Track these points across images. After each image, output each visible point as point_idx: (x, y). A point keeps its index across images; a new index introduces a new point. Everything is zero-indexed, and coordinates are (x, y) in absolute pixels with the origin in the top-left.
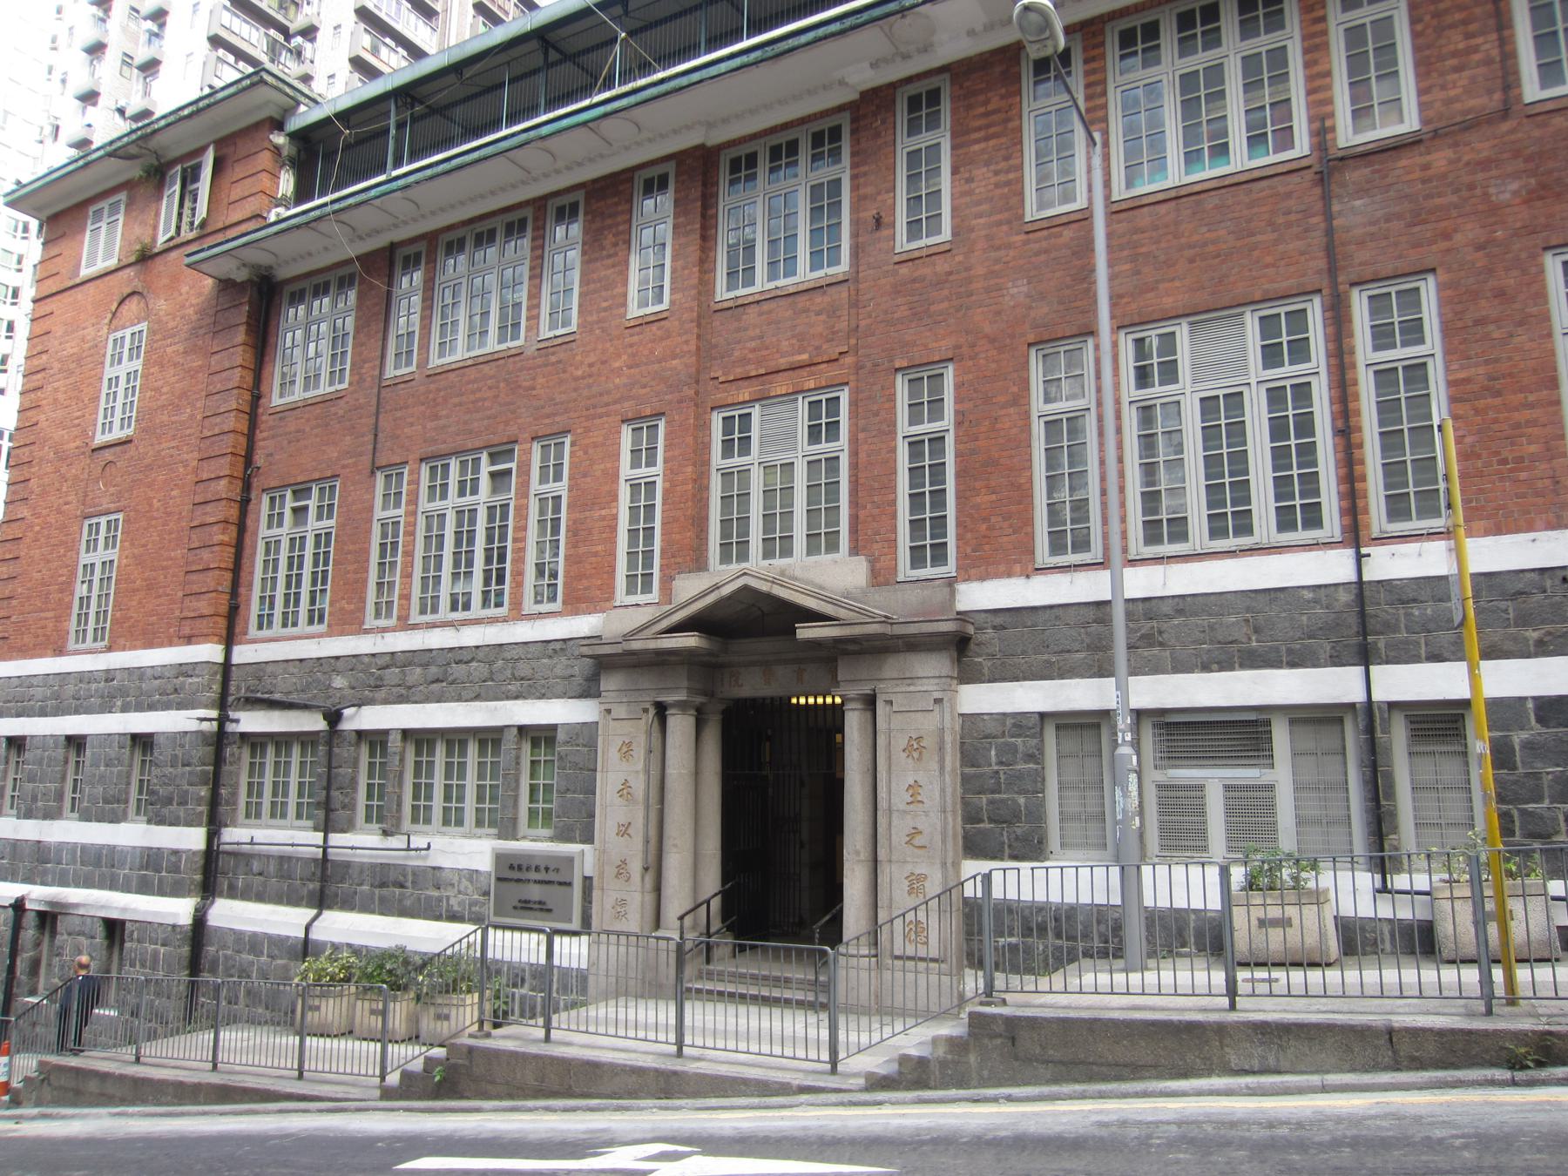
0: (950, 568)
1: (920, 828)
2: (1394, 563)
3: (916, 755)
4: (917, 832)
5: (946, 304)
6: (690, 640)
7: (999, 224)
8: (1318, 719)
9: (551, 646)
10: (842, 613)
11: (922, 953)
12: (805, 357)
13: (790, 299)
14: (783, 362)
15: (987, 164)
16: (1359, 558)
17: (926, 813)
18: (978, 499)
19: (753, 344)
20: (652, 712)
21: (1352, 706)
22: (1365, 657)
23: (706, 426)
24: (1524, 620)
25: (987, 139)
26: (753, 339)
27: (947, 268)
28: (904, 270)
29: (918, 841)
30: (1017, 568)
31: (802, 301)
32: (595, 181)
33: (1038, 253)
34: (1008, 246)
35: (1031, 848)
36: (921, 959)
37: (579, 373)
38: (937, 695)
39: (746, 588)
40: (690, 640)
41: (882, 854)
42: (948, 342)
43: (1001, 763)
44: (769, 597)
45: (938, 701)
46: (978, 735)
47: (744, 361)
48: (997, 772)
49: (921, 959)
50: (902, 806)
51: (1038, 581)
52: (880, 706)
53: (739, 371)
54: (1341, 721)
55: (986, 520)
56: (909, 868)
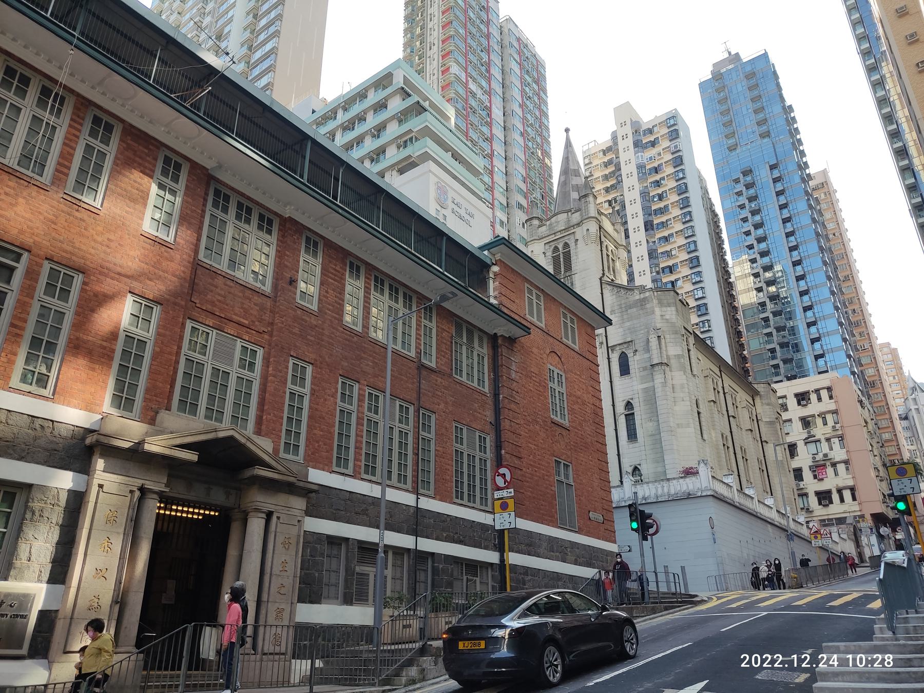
0: (300, 458)
2: (427, 504)
4: (283, 586)
5: (312, 339)
6: (191, 456)
7: (335, 318)
8: (399, 552)
9: (40, 422)
10: (280, 467)
11: (277, 649)
12: (247, 322)
13: (242, 288)
14: (235, 318)
15: (333, 290)
16: (418, 498)
18: (315, 431)
19: (220, 298)
20: (137, 494)
21: (408, 550)
22: (416, 533)
23: (183, 325)
24: (443, 530)
25: (334, 280)
26: (219, 294)
27: (315, 323)
28: (299, 312)
30: (326, 468)
31: (248, 293)
32: (131, 125)
33: (346, 339)
34: (337, 330)
36: (277, 654)
37: (99, 239)
38: (300, 518)
39: (231, 438)
40: (191, 456)
41: (265, 597)
42: (313, 356)
43: (311, 556)
44: (243, 446)
46: (313, 541)
47: (213, 303)
49: (277, 654)
50: (278, 573)
51: (333, 475)
52: (274, 519)
53: (209, 307)
54: (403, 555)
55: (318, 442)
56: (277, 605)
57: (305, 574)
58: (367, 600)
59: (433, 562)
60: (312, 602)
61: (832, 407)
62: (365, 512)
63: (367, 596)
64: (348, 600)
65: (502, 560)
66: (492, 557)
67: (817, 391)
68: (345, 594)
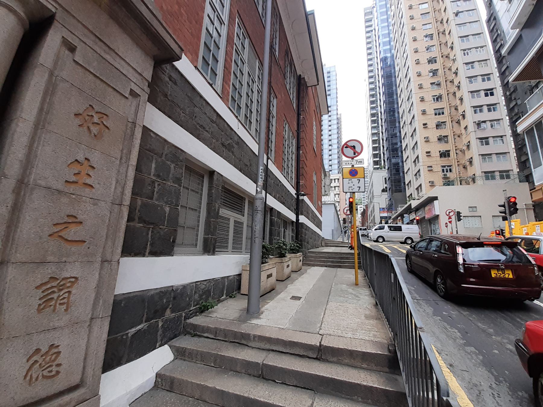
1: (81, 217)
3: (95, 130)
4: (73, 220)
17: (95, 201)
29: (72, 232)
35: (164, 247)
43: (158, 176)
45: (133, 94)
48: (153, 182)
50: (59, 185)
52: (52, 41)
57: (144, 205)
58: (227, 247)
59: (271, 216)
60: (155, 253)
61: (338, 185)
62: (229, 148)
63: (227, 243)
64: (210, 248)
65: (298, 219)
66: (292, 216)
67: (335, 179)
68: (206, 241)
